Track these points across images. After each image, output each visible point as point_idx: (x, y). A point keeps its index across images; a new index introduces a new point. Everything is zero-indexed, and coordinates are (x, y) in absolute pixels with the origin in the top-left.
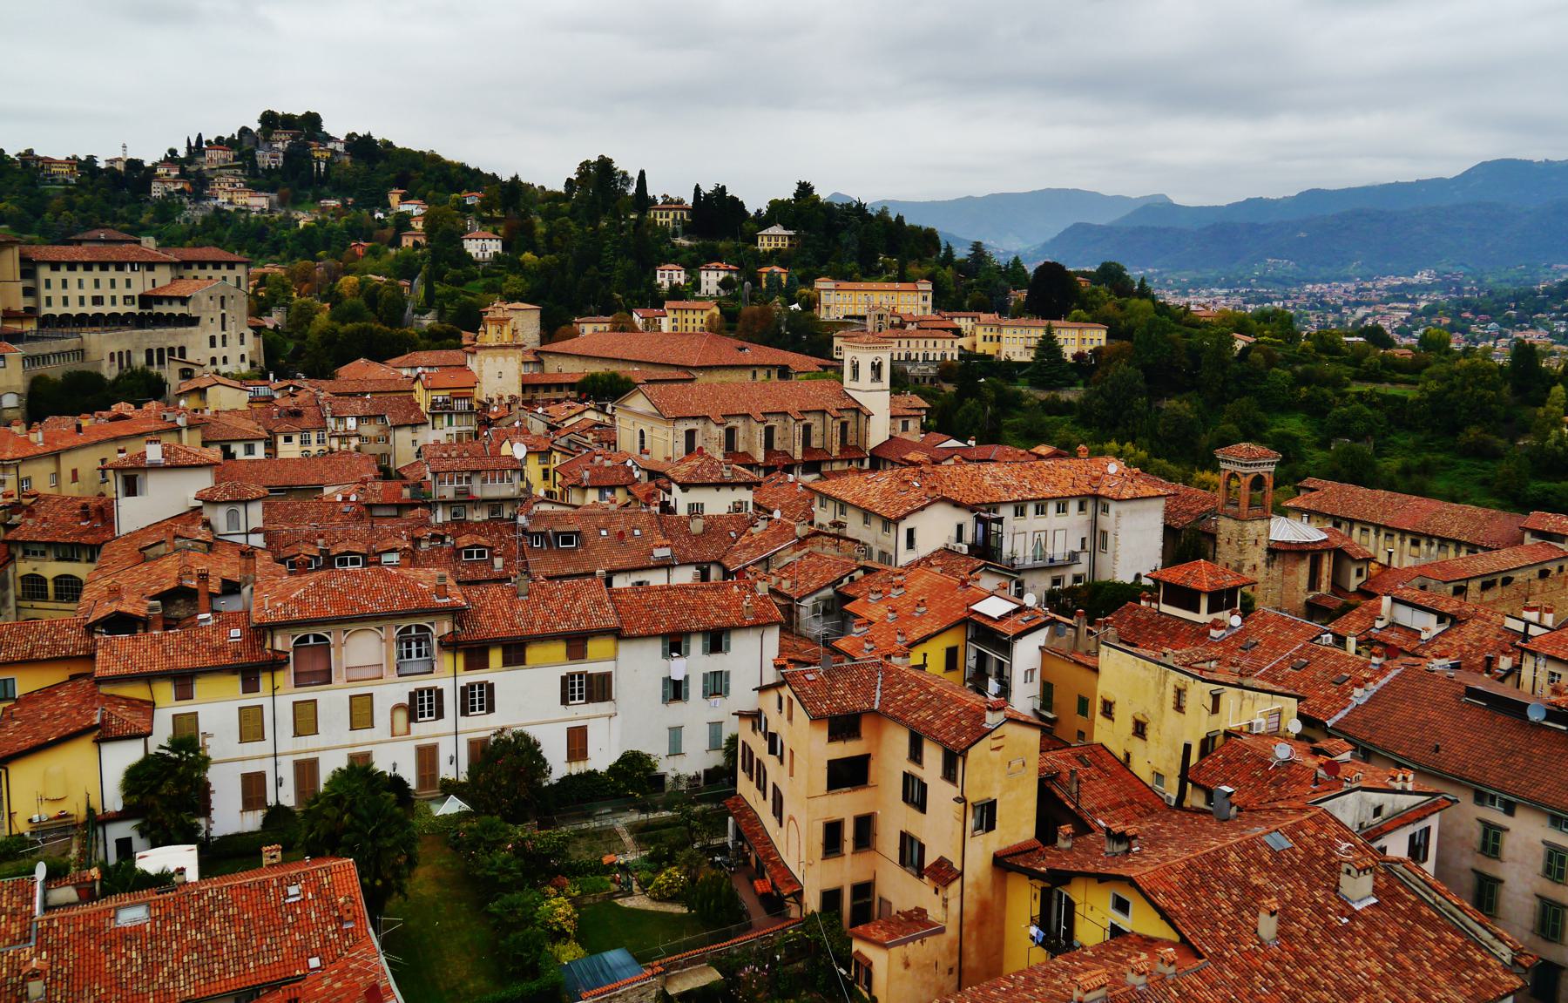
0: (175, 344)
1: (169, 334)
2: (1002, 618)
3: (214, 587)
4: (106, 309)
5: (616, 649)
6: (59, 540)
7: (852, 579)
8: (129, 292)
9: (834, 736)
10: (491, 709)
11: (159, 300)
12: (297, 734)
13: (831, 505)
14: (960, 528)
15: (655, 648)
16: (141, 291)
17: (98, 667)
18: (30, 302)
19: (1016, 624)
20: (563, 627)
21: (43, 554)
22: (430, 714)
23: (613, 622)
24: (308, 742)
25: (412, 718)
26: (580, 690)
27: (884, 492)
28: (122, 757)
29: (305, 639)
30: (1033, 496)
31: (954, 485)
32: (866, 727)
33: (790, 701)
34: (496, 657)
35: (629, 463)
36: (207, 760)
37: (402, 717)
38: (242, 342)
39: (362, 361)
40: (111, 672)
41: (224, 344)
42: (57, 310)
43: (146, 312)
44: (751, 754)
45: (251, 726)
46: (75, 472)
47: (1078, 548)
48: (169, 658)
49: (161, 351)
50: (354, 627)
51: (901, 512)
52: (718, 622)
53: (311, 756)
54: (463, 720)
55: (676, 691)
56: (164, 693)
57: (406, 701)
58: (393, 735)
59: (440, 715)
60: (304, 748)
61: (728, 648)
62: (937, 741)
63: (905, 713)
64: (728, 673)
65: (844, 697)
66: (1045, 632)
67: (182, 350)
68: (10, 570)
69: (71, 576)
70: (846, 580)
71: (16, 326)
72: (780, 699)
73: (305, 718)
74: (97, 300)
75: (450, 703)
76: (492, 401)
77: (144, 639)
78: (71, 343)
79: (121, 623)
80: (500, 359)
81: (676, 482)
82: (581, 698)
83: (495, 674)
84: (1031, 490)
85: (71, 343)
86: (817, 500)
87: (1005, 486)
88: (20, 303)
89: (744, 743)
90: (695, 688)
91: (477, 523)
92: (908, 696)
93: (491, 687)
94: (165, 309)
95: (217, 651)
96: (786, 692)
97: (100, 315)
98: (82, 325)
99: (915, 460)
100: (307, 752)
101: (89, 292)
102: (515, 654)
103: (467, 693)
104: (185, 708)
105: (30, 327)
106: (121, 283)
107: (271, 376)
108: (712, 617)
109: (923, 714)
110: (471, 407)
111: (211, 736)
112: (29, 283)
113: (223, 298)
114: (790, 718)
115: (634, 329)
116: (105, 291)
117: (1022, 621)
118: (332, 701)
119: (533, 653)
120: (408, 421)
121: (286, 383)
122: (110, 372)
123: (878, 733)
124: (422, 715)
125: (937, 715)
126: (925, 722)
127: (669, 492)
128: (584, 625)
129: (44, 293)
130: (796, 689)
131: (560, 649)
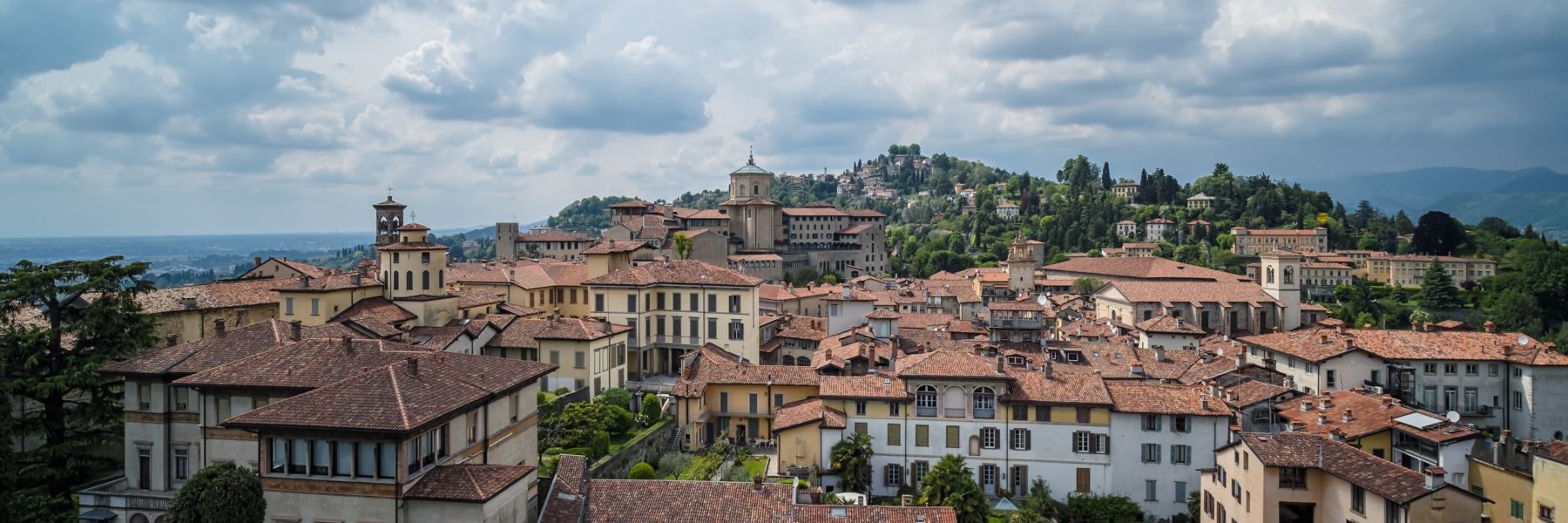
0: (850, 259)
1: (848, 254)
2: (1425, 429)
3: (877, 359)
4: (818, 241)
5: (1110, 419)
6: (801, 337)
7: (1283, 398)
8: (829, 232)
9: (1284, 483)
10: (1028, 447)
11: (843, 235)
12: (917, 445)
13: (1260, 352)
14: (1374, 373)
15: (1136, 423)
16: (834, 231)
17: (821, 390)
18: (786, 237)
19: (1441, 434)
20: (1074, 399)
21: (793, 345)
22: (992, 445)
23: (1108, 400)
24: (923, 451)
25: (981, 445)
26: (1086, 444)
27: (1305, 344)
28: (831, 439)
29: (923, 388)
30: (1442, 356)
31: (1366, 343)
32: (1310, 480)
33: (1246, 455)
34: (1032, 413)
35: (1109, 323)
36: (872, 453)
37: (975, 444)
38: (882, 259)
39: (942, 272)
40: (827, 394)
41: (873, 260)
42: (798, 241)
43: (837, 242)
44: (1212, 499)
45: (894, 436)
46: (806, 310)
47: (1491, 404)
48: (855, 390)
49: (843, 262)
50: (950, 384)
51: (1322, 357)
52: (1182, 410)
53: (924, 459)
54: (1011, 452)
55: (1150, 454)
56: (851, 409)
57: (978, 434)
58: (970, 454)
59: (998, 446)
60: (921, 454)
61: (1189, 430)
62: (1377, 494)
63: (1348, 472)
64: (1189, 448)
65: (1291, 455)
66: (1471, 443)
67: (853, 263)
68: (779, 352)
69: (804, 357)
70: (1279, 399)
71: (779, 248)
72: (1237, 455)
73: (922, 437)
74: (815, 236)
75: (1004, 439)
76: (1018, 290)
77: (843, 379)
78: (802, 256)
79: (831, 370)
80: (1022, 269)
81: (1143, 330)
82: (1086, 449)
83: (1031, 424)
84: (1440, 352)
85: (802, 256)
86: (1249, 349)
87: (1414, 348)
88: (782, 237)
89: (1206, 492)
90: (1166, 455)
91: (1016, 344)
92: (1348, 461)
93: (1028, 433)
94: (844, 240)
95: (877, 389)
96: (1243, 448)
97: (816, 244)
98: (809, 249)
99: (1330, 324)
100: (923, 456)
101: (811, 232)
102: (1044, 411)
103: (1014, 434)
104: (861, 420)
105: (785, 248)
106: (826, 227)
107: (896, 276)
108: (1177, 406)
109: (1364, 474)
110: (1005, 293)
111: (873, 438)
112: (786, 227)
113: (873, 235)
114: (1246, 467)
115: (1101, 256)
116: (819, 231)
117: (1446, 433)
118: (937, 427)
119: (1055, 414)
120: (969, 301)
121: (903, 279)
122: (820, 271)
123: (1322, 489)
124: (987, 445)
125: (1376, 475)
126: (1365, 479)
127: (1138, 338)
128: (1088, 400)
129: (792, 232)
130: (1251, 445)
131: (1072, 414)
